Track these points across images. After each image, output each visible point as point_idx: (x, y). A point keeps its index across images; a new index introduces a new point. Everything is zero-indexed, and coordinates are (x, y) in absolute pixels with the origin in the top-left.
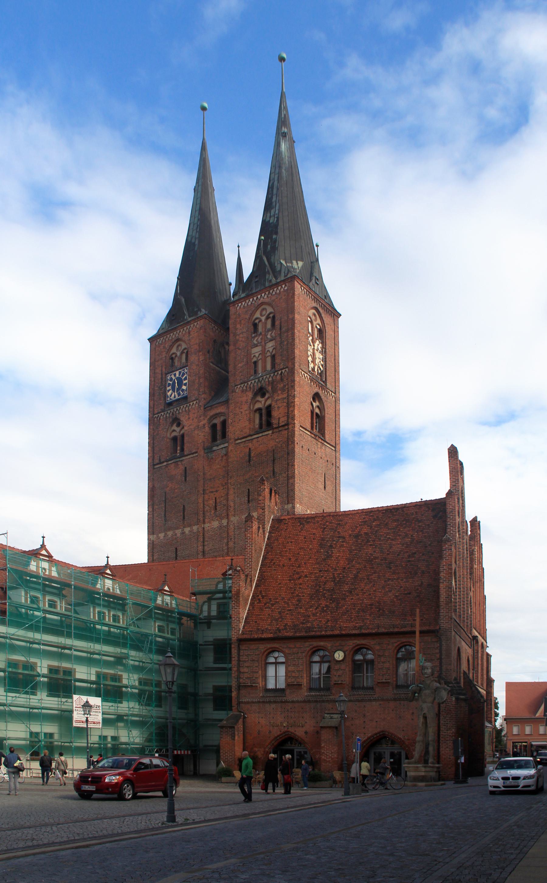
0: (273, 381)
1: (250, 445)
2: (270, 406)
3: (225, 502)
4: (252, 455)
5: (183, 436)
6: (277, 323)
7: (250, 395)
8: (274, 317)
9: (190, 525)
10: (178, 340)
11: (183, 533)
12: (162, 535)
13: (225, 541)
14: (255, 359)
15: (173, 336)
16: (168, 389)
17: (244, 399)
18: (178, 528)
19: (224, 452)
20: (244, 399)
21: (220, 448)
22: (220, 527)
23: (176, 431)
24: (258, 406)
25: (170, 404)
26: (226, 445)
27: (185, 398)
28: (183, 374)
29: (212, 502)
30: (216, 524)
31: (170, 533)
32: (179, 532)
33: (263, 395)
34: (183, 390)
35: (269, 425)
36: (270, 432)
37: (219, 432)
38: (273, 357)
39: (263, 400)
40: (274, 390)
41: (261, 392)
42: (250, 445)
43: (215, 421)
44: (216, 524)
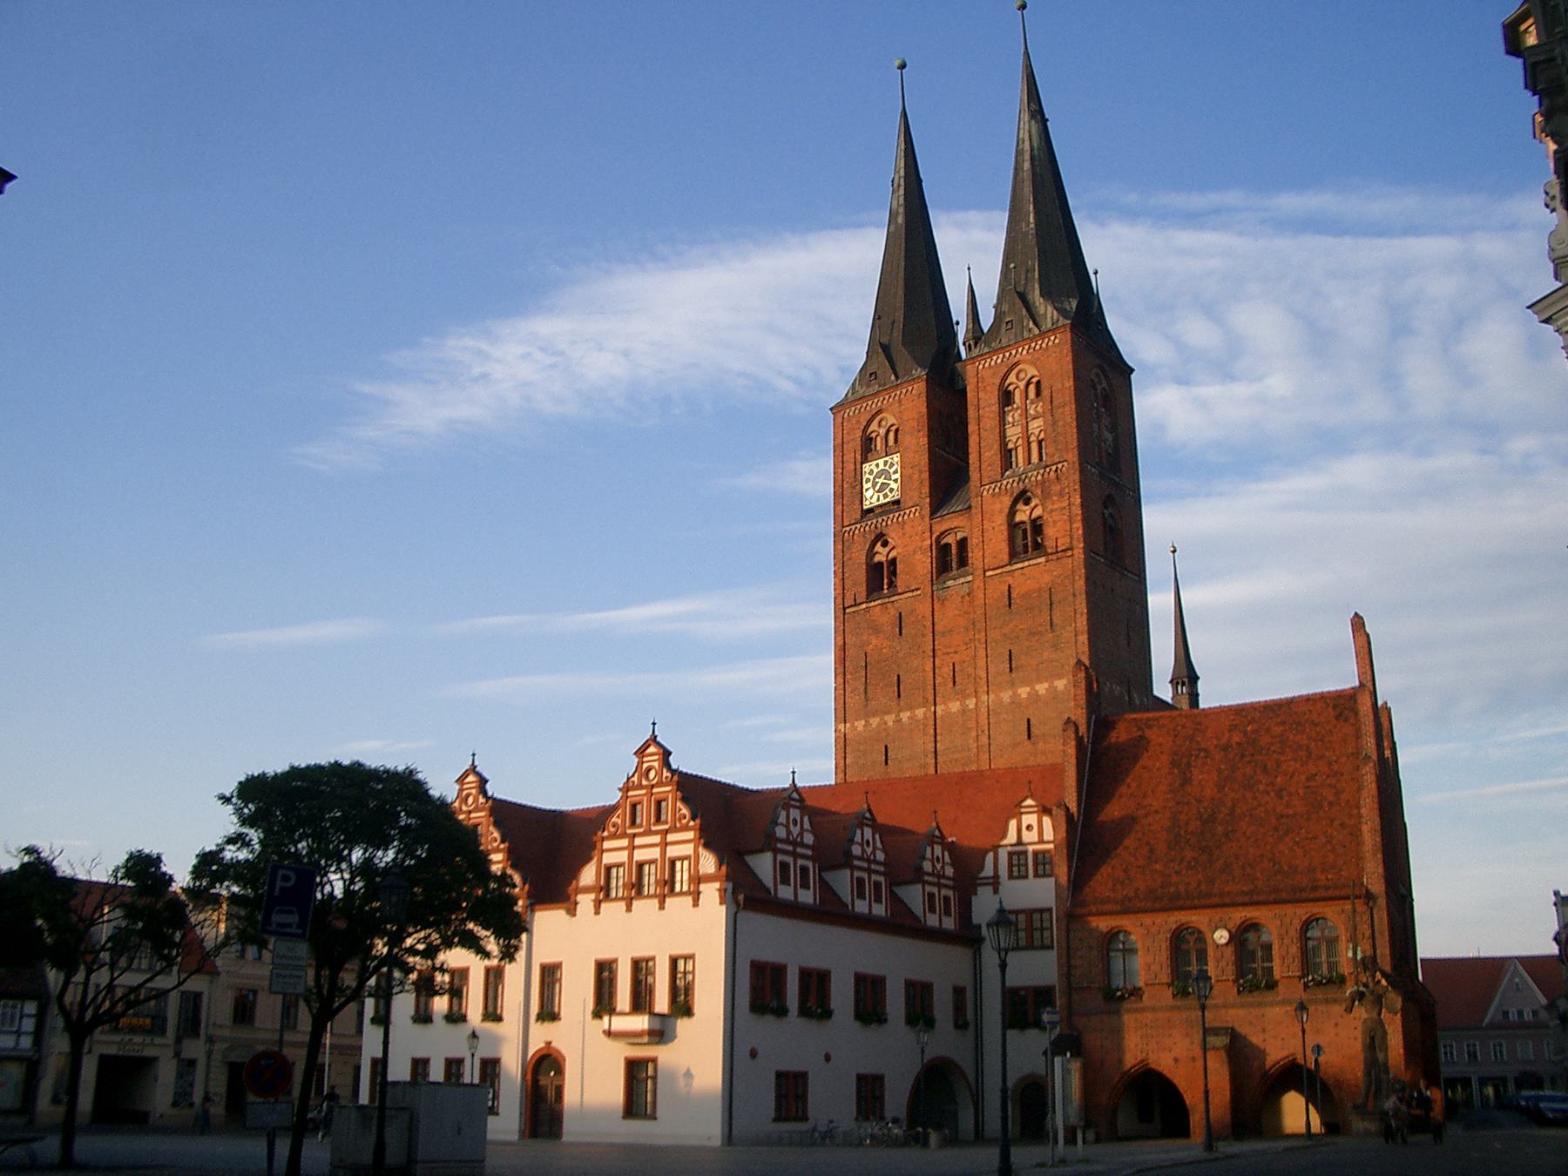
0: (1044, 481)
1: (1010, 580)
2: (1040, 517)
3: (970, 670)
4: (1014, 595)
5: (893, 562)
6: (1045, 393)
7: (1007, 501)
8: (1038, 383)
9: (911, 708)
10: (879, 412)
11: (899, 721)
12: (860, 724)
13: (974, 734)
14: (1010, 446)
15: (872, 406)
16: (865, 486)
17: (998, 506)
18: (888, 713)
19: (966, 589)
20: (998, 506)
21: (956, 584)
22: (964, 711)
23: (881, 555)
24: (1018, 518)
25: (871, 510)
26: (970, 578)
27: (897, 502)
28: (892, 465)
29: (947, 671)
30: (955, 706)
31: (875, 721)
32: (890, 719)
33: (1027, 503)
34: (892, 490)
35: (1038, 547)
36: (1042, 560)
37: (950, 558)
38: (1040, 442)
39: (1027, 508)
40: (1046, 496)
41: (1023, 497)
42: (1010, 580)
43: (950, 539)
44: (955, 706)
